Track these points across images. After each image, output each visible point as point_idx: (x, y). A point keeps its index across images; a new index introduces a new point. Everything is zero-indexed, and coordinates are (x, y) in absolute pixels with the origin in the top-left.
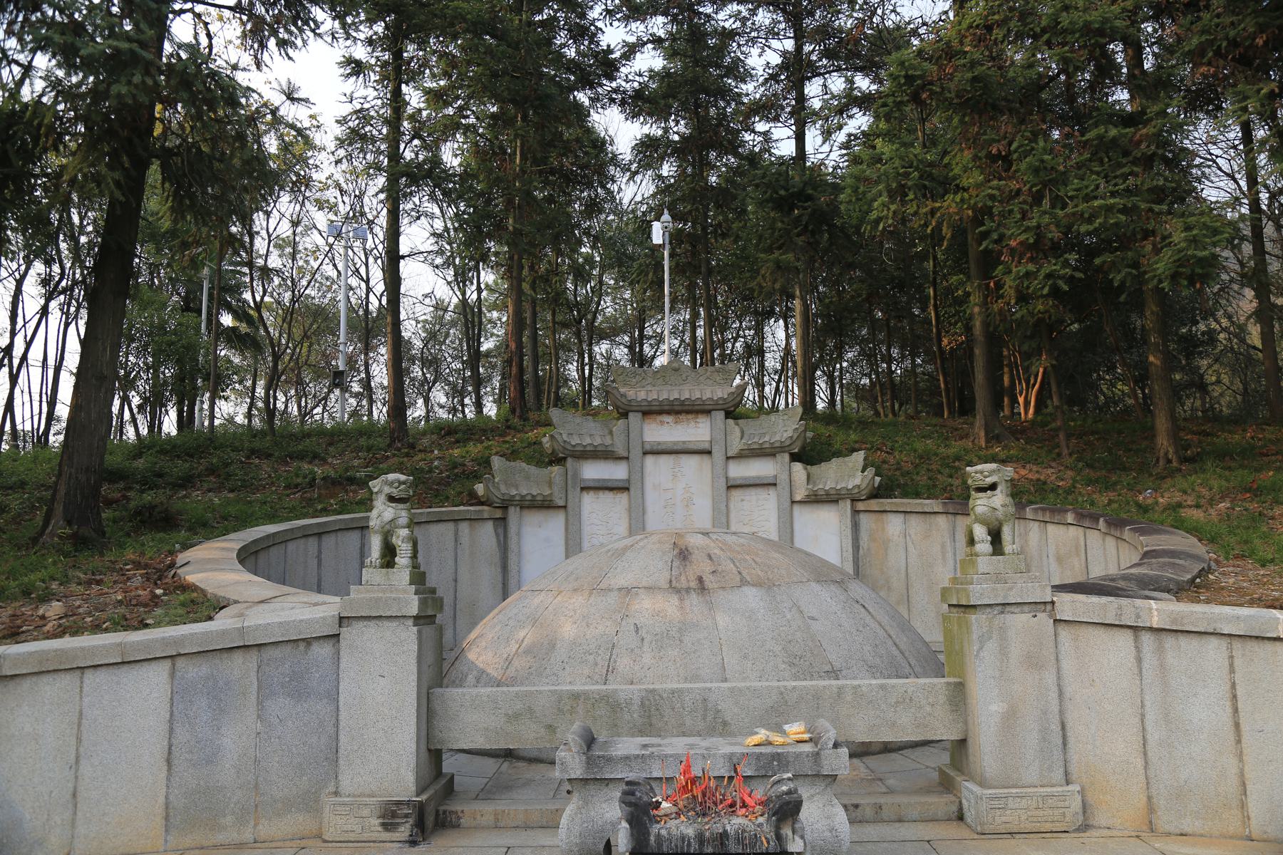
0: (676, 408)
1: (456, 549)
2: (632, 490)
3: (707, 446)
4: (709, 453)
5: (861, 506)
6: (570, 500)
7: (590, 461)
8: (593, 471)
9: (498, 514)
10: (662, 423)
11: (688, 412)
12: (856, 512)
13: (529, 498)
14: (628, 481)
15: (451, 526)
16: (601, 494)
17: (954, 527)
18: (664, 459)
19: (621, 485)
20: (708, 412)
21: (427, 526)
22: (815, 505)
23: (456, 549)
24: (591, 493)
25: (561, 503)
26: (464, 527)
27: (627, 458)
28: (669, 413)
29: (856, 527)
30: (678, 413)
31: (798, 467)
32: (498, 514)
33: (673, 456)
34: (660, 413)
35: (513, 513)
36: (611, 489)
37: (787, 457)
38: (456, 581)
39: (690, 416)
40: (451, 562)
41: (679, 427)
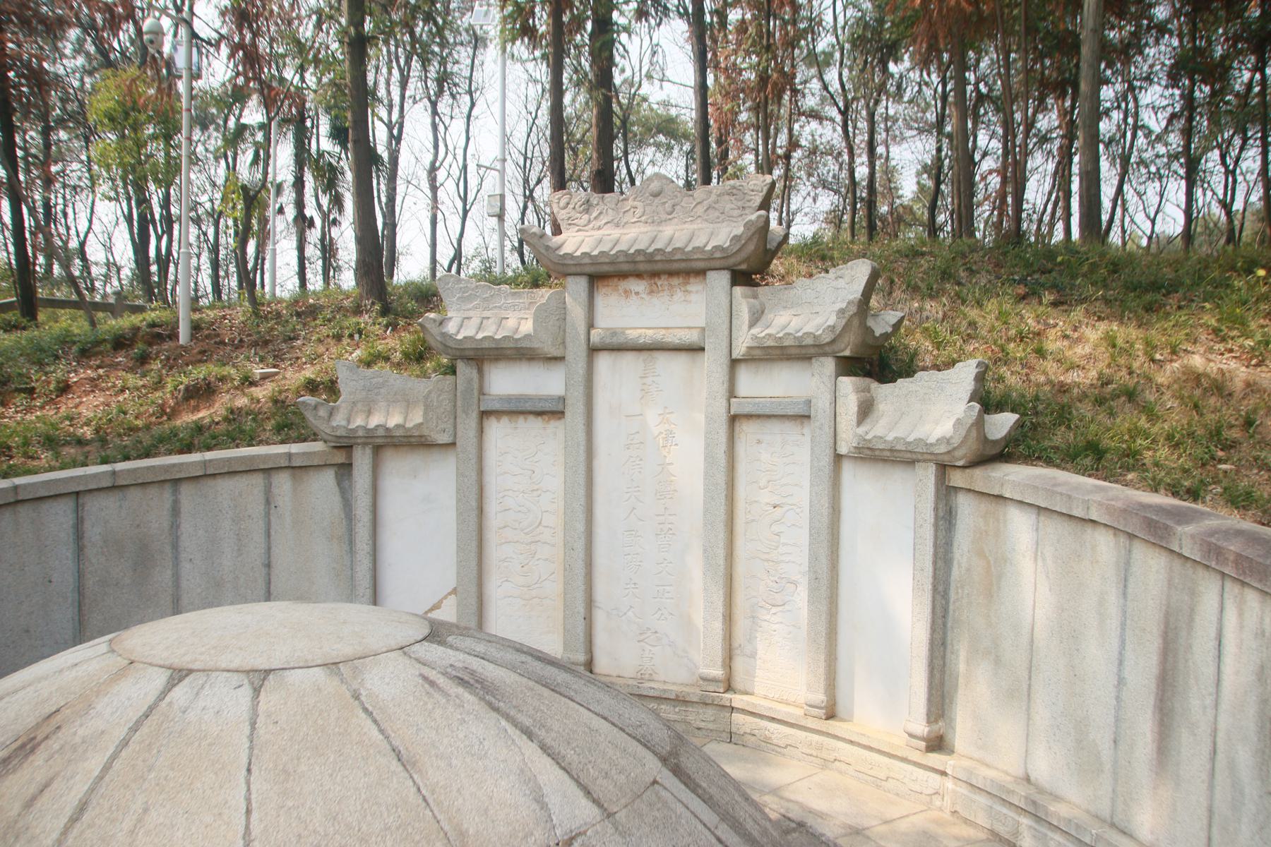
0: (642, 267)
1: (268, 514)
2: (568, 414)
3: (691, 337)
4: (703, 349)
5: (957, 479)
6: (459, 434)
7: (501, 365)
8: (505, 382)
9: (340, 458)
10: (627, 293)
11: (671, 274)
12: (945, 492)
13: (381, 432)
14: (562, 399)
15: (258, 480)
16: (521, 419)
17: (1128, 563)
18: (628, 359)
19: (548, 406)
20: (701, 273)
21: (211, 482)
22: (881, 465)
23: (268, 514)
24: (505, 420)
25: (444, 438)
26: (283, 482)
27: (561, 359)
28: (639, 275)
29: (945, 518)
30: (655, 275)
31: (848, 384)
32: (340, 458)
33: (645, 355)
34: (623, 276)
35: (362, 460)
36: (539, 414)
37: (829, 365)
38: (268, 566)
39: (675, 281)
40: (258, 537)
41: (655, 300)
